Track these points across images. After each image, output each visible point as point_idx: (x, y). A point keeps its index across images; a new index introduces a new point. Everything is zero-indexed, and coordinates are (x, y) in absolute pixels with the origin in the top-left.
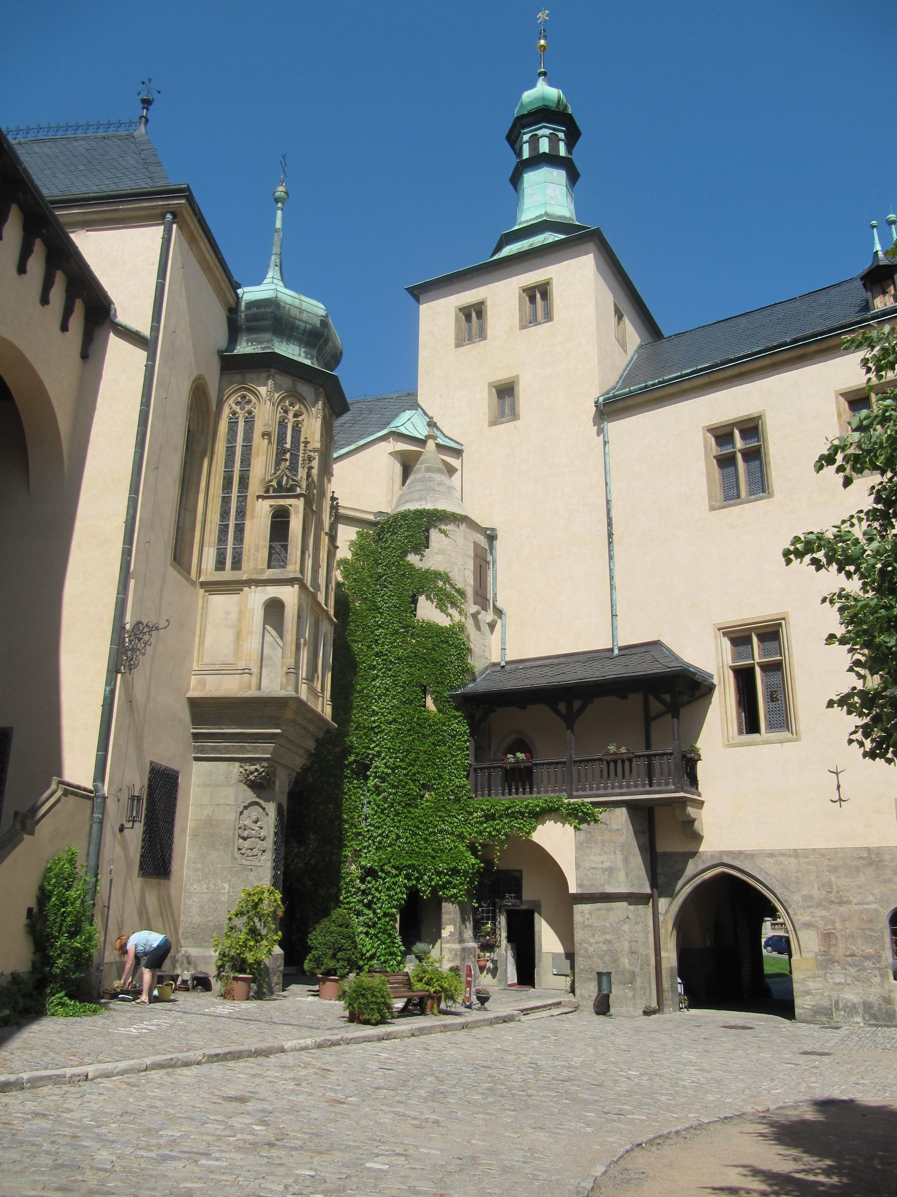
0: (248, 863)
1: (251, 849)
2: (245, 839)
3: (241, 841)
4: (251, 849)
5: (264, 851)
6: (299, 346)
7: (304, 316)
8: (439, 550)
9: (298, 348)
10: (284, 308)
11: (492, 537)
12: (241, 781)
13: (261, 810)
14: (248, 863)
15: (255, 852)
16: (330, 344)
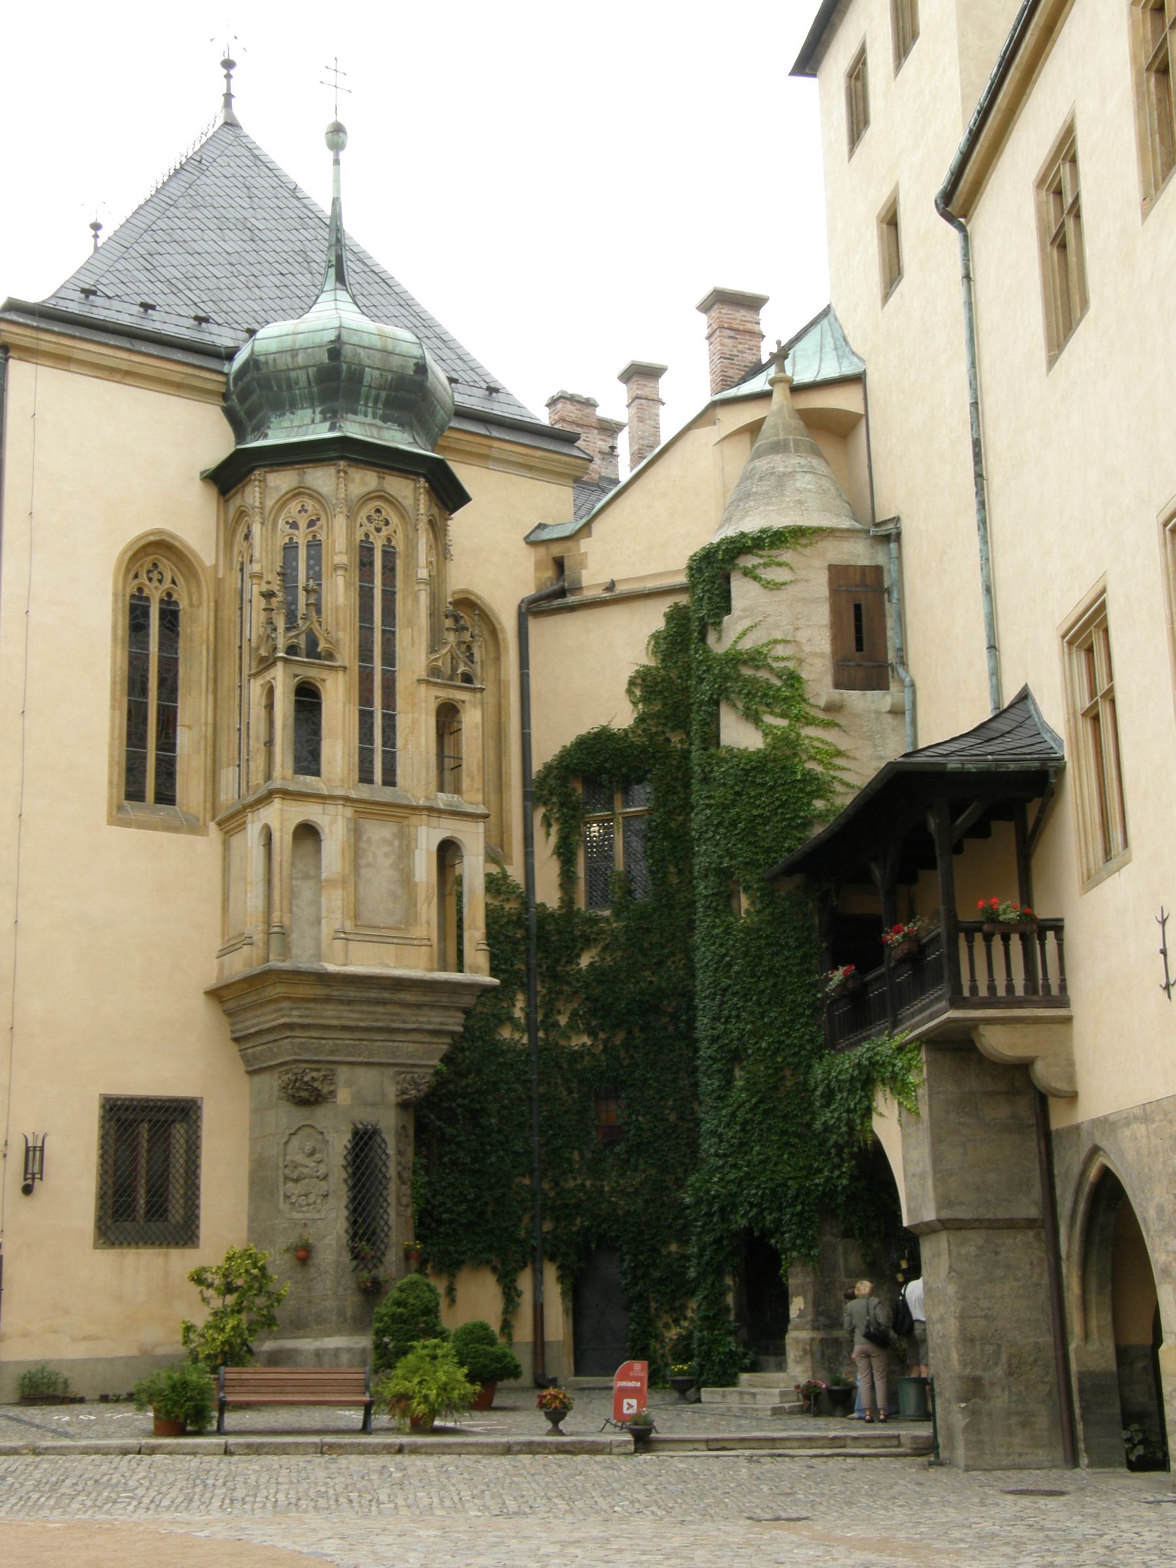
0: (300, 1216)
1: (306, 1195)
2: (297, 1181)
3: (290, 1184)
4: (306, 1195)
5: (326, 1196)
6: (312, 406)
7: (301, 359)
8: (744, 610)
9: (309, 411)
10: (267, 363)
11: (888, 535)
12: (280, 1098)
13: (319, 1137)
14: (300, 1216)
15: (312, 1198)
16: (370, 375)
